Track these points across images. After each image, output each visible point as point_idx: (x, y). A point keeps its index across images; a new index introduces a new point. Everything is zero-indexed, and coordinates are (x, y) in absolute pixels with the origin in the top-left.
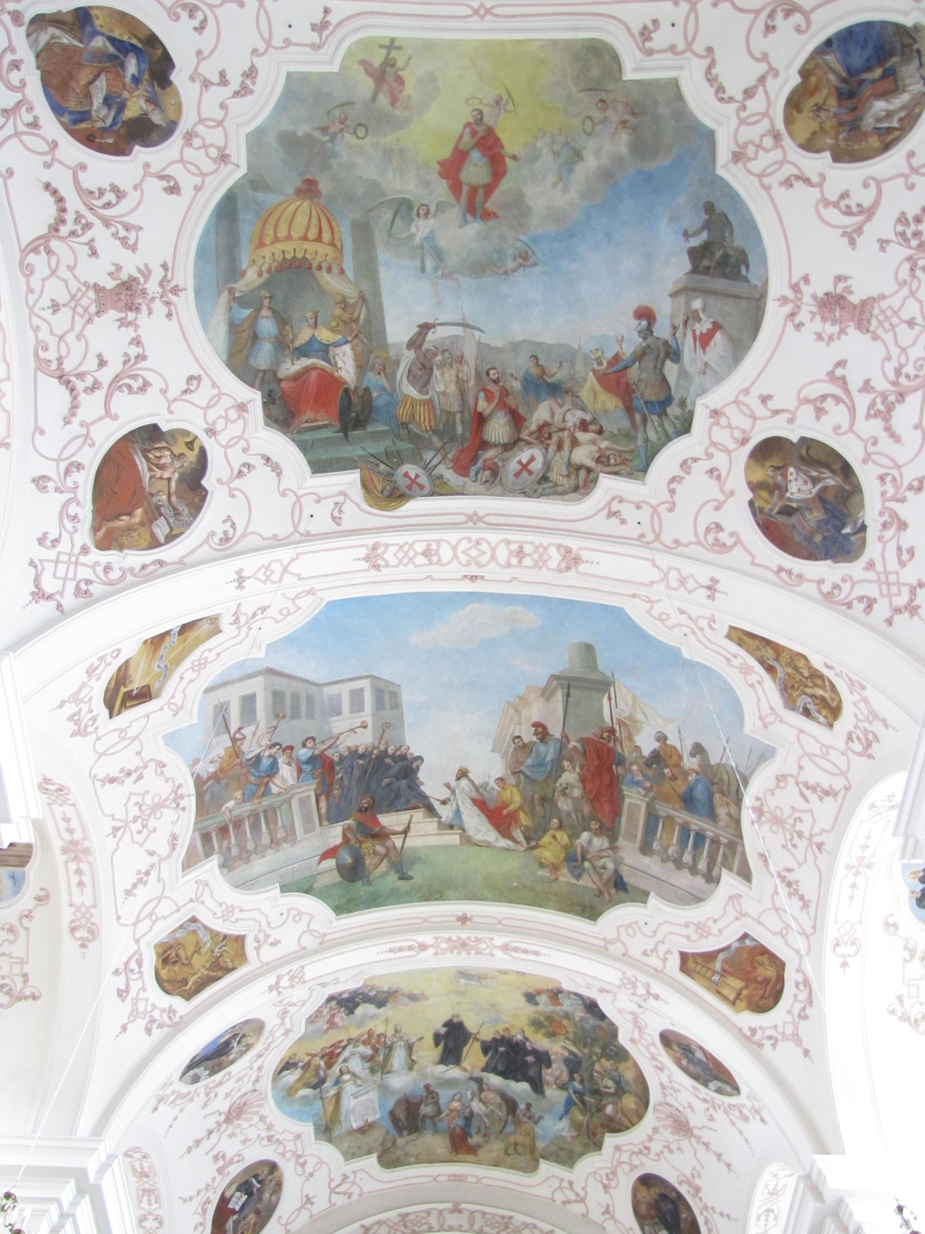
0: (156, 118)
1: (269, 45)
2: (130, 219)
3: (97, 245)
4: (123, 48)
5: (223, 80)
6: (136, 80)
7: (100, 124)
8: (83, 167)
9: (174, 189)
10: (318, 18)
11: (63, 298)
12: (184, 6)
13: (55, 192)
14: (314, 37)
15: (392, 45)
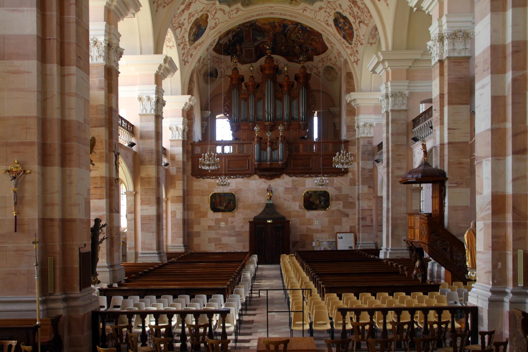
0: (339, 16)
1: (315, 11)
2: (349, 8)
3: (356, 12)
4: (340, 28)
5: (326, 12)
6: (340, 23)
7: (348, 24)
8: (353, 22)
9: (340, 5)
10: (305, 12)
11: (365, 16)
12: (329, 25)
13: (359, 25)
14: (306, 9)
15: (291, 4)
